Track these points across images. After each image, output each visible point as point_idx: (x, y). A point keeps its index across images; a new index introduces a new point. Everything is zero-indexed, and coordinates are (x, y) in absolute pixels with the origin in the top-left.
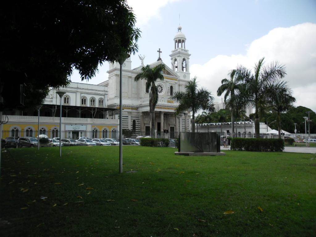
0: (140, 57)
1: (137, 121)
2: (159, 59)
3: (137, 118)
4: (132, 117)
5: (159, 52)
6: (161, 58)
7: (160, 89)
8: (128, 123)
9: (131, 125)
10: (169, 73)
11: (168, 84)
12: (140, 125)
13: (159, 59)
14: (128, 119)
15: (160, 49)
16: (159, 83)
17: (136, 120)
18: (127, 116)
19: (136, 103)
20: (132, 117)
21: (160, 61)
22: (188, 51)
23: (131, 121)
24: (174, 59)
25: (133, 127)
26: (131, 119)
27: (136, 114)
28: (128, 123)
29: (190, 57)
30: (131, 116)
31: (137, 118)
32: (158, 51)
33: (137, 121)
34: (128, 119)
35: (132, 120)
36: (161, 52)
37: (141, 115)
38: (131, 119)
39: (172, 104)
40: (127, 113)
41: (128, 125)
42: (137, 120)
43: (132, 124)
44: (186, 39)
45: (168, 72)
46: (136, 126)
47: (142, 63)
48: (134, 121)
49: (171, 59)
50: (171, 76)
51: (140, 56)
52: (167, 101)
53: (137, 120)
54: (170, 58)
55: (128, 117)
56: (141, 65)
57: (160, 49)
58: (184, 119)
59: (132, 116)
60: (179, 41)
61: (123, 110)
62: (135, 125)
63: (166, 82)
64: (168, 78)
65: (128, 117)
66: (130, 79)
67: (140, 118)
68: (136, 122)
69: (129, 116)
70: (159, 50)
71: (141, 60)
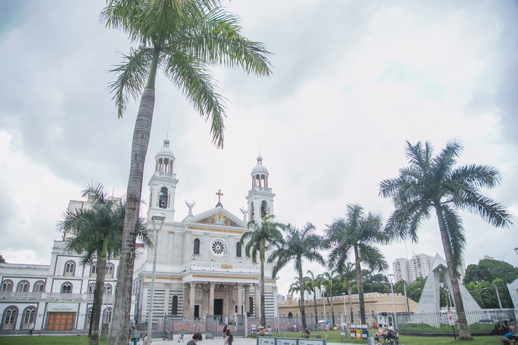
0: (186, 203)
1: (180, 298)
2: (219, 204)
4: (170, 291)
5: (219, 194)
6: (221, 202)
7: (220, 248)
8: (164, 300)
10: (234, 223)
11: (232, 240)
13: (219, 204)
14: (164, 294)
15: (220, 191)
16: (216, 239)
17: (179, 296)
18: (164, 289)
19: (177, 269)
20: (170, 291)
21: (219, 207)
22: (272, 189)
23: (170, 297)
24: (250, 202)
25: (173, 307)
26: (170, 294)
27: (177, 286)
28: (164, 300)
29: (274, 198)
30: (169, 290)
32: (217, 194)
33: (180, 298)
34: (164, 294)
35: (172, 296)
36: (222, 194)
37: (184, 287)
38: (170, 294)
39: (230, 270)
40: (163, 285)
41: (163, 304)
44: (268, 174)
45: (232, 222)
47: (190, 211)
48: (175, 298)
49: (248, 203)
50: (241, 228)
51: (186, 202)
52: (220, 266)
54: (247, 201)
55: (164, 291)
56: (188, 214)
57: (220, 191)
58: (254, 292)
59: (171, 290)
60: (258, 177)
61: (259, 275)
63: (229, 237)
64: (232, 232)
65: (164, 291)
66: (171, 235)
68: (179, 299)
69: (166, 290)
70: (218, 192)
71: (189, 208)
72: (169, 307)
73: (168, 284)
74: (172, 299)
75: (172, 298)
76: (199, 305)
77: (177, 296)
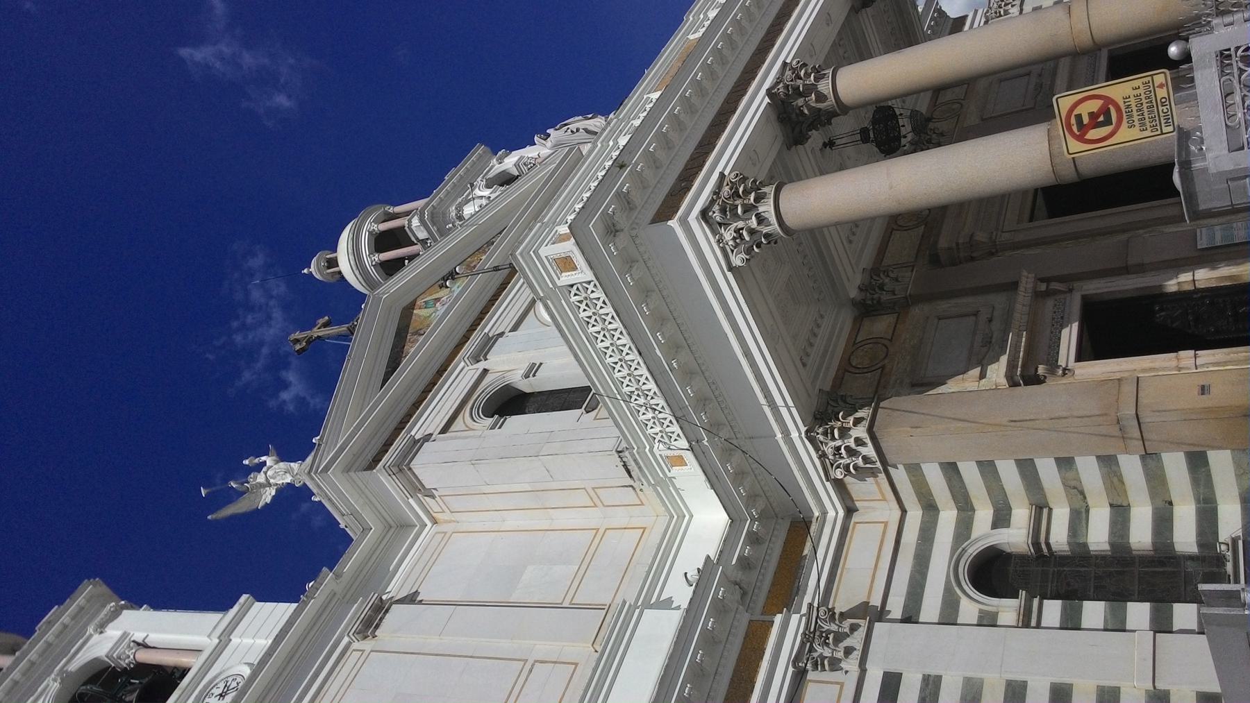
1: (1001, 519)
3: (948, 517)
9: (1071, 622)
12: (1065, 463)
17: (984, 533)
20: (910, 617)
23: (988, 620)
25: (1117, 596)
26: (949, 617)
31: (948, 517)
33: (1001, 519)
35: (971, 606)
38: (949, 617)
42: (984, 515)
43: (1053, 610)
46: (1098, 536)
53: (984, 515)
59: (896, 607)
62: (1080, 556)
67: (934, 476)
68: (1015, 537)
72: (1117, 625)
73: (810, 637)
74: (1008, 609)
75: (993, 603)
76: (1084, 298)
77: (973, 550)
